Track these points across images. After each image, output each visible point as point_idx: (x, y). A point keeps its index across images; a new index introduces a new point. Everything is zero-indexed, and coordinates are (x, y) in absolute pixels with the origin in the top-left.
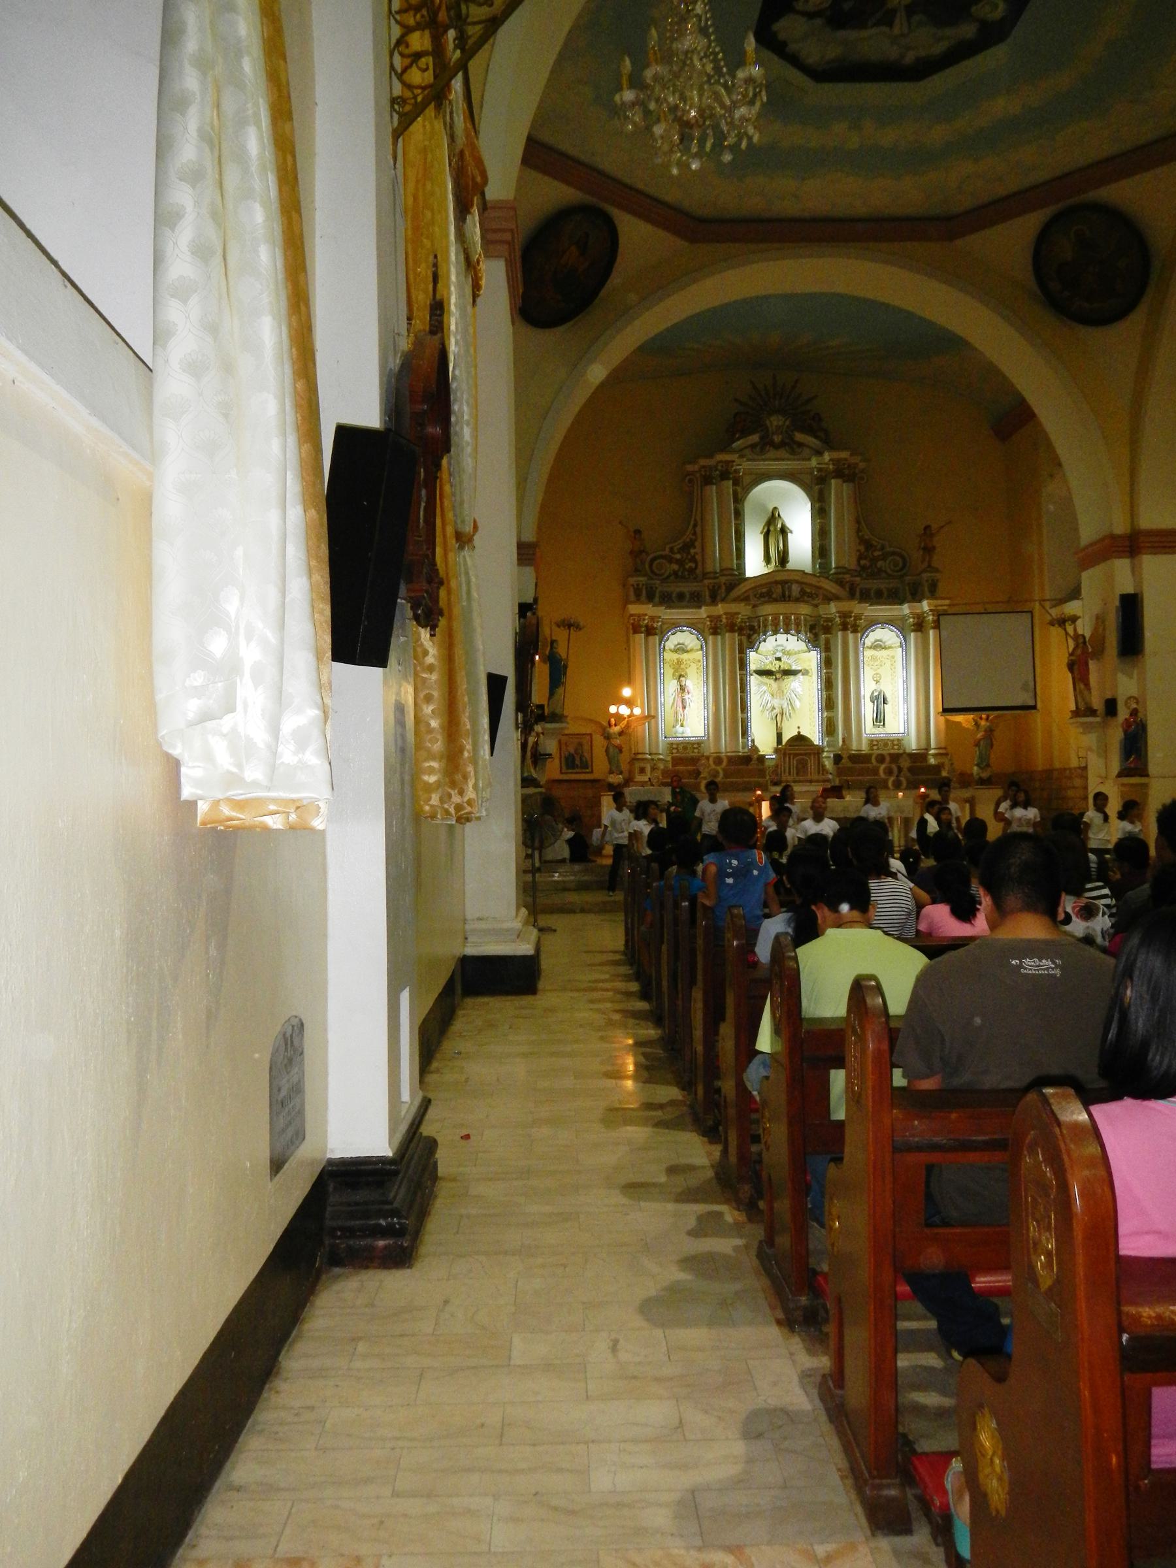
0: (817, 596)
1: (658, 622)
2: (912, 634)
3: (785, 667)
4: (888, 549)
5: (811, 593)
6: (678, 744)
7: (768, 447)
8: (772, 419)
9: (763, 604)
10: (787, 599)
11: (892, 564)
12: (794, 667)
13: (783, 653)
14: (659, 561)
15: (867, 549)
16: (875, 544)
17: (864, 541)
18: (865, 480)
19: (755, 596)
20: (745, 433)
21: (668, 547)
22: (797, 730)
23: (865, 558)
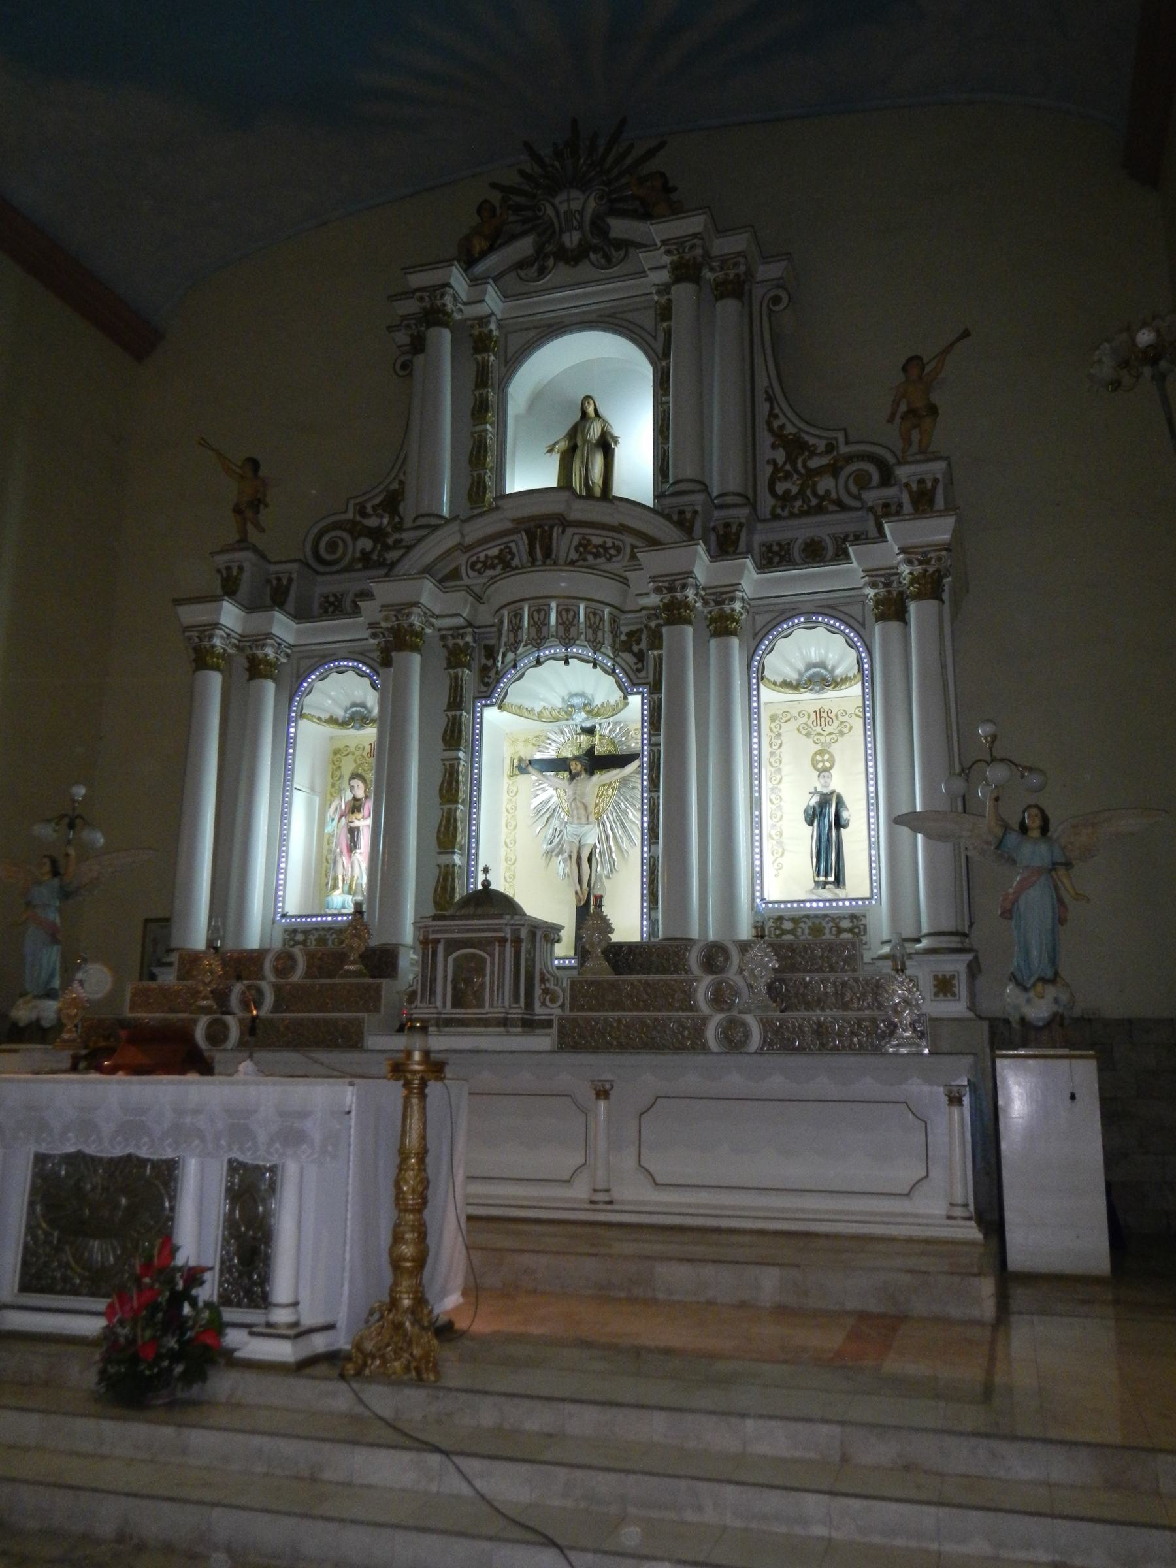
0: (619, 550)
1: (264, 646)
2: (878, 628)
3: (601, 749)
4: (844, 449)
5: (603, 546)
6: (306, 932)
7: (551, 262)
8: (557, 201)
9: (493, 580)
10: (539, 563)
11: (851, 481)
12: (622, 750)
13: (589, 712)
14: (333, 534)
15: (791, 459)
16: (811, 441)
17: (780, 439)
18: (782, 306)
19: (473, 566)
20: (496, 240)
21: (352, 502)
22: (481, 877)
23: (788, 476)
